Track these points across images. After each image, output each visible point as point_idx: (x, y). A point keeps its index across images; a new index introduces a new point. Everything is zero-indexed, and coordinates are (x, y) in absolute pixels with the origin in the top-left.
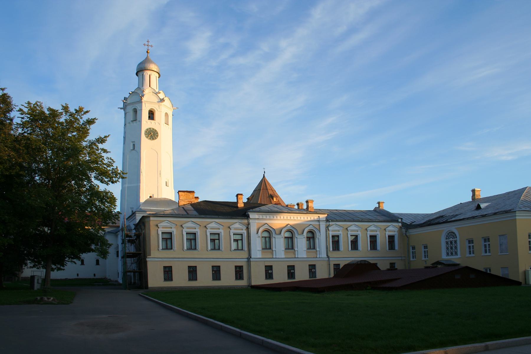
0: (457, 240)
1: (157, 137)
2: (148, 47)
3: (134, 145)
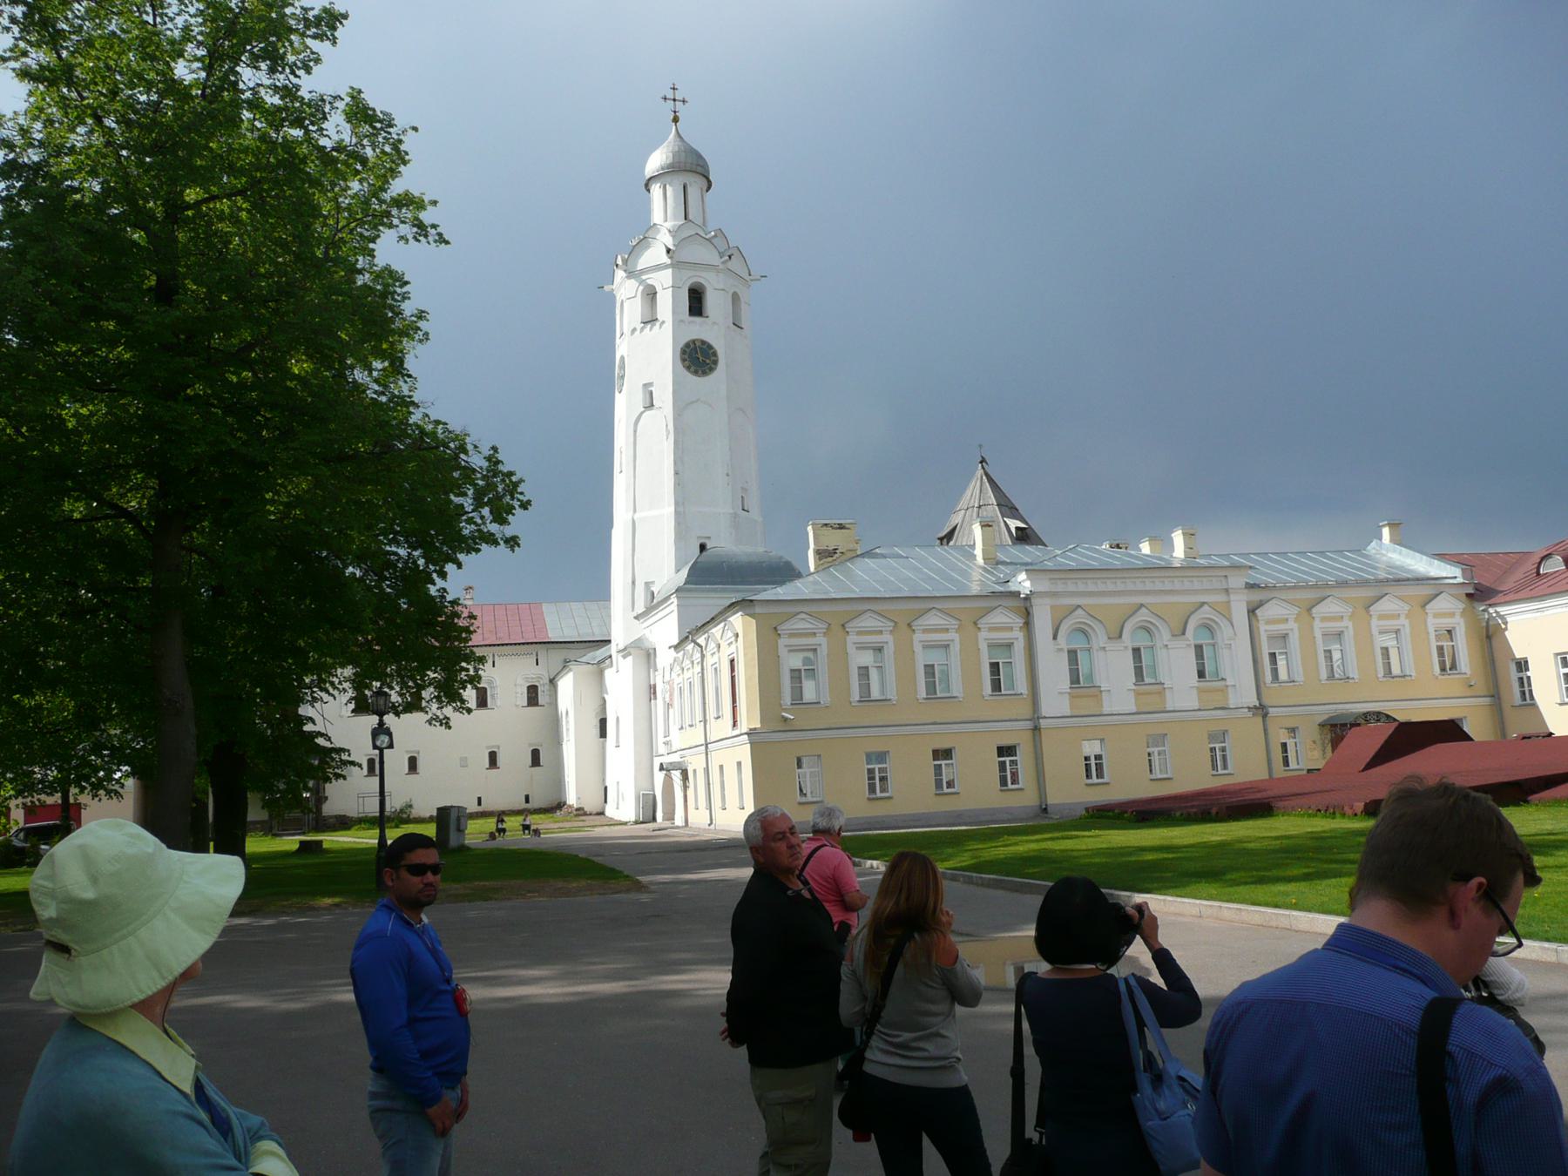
1: (713, 366)
2: (675, 105)
3: (651, 393)
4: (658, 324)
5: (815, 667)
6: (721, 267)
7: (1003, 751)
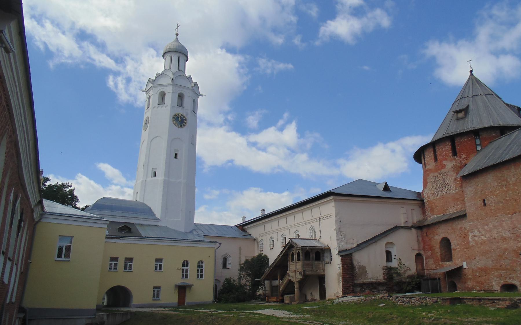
1: (185, 124)
4: (165, 105)
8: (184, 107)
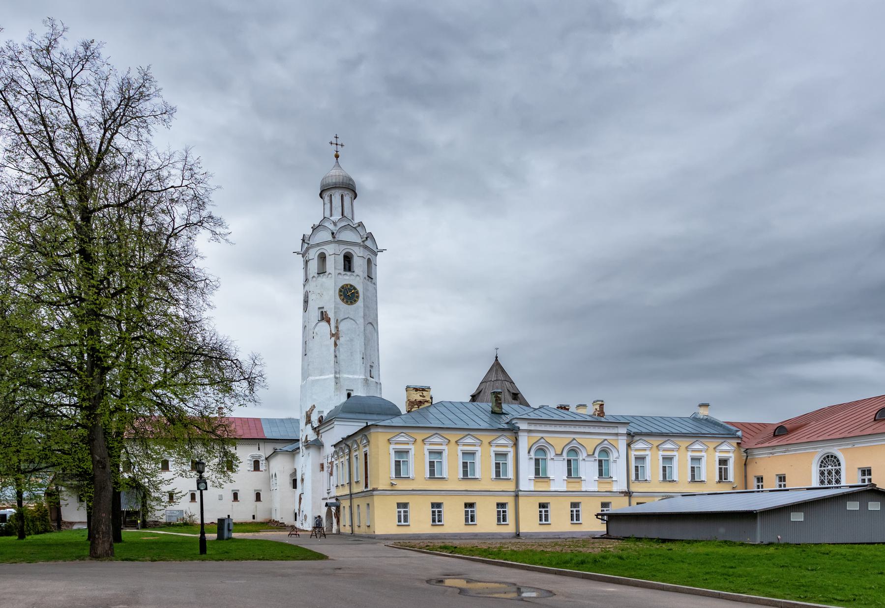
0: (840, 469)
5: (408, 460)
6: (362, 244)
7: (501, 505)
8: (354, 272)
